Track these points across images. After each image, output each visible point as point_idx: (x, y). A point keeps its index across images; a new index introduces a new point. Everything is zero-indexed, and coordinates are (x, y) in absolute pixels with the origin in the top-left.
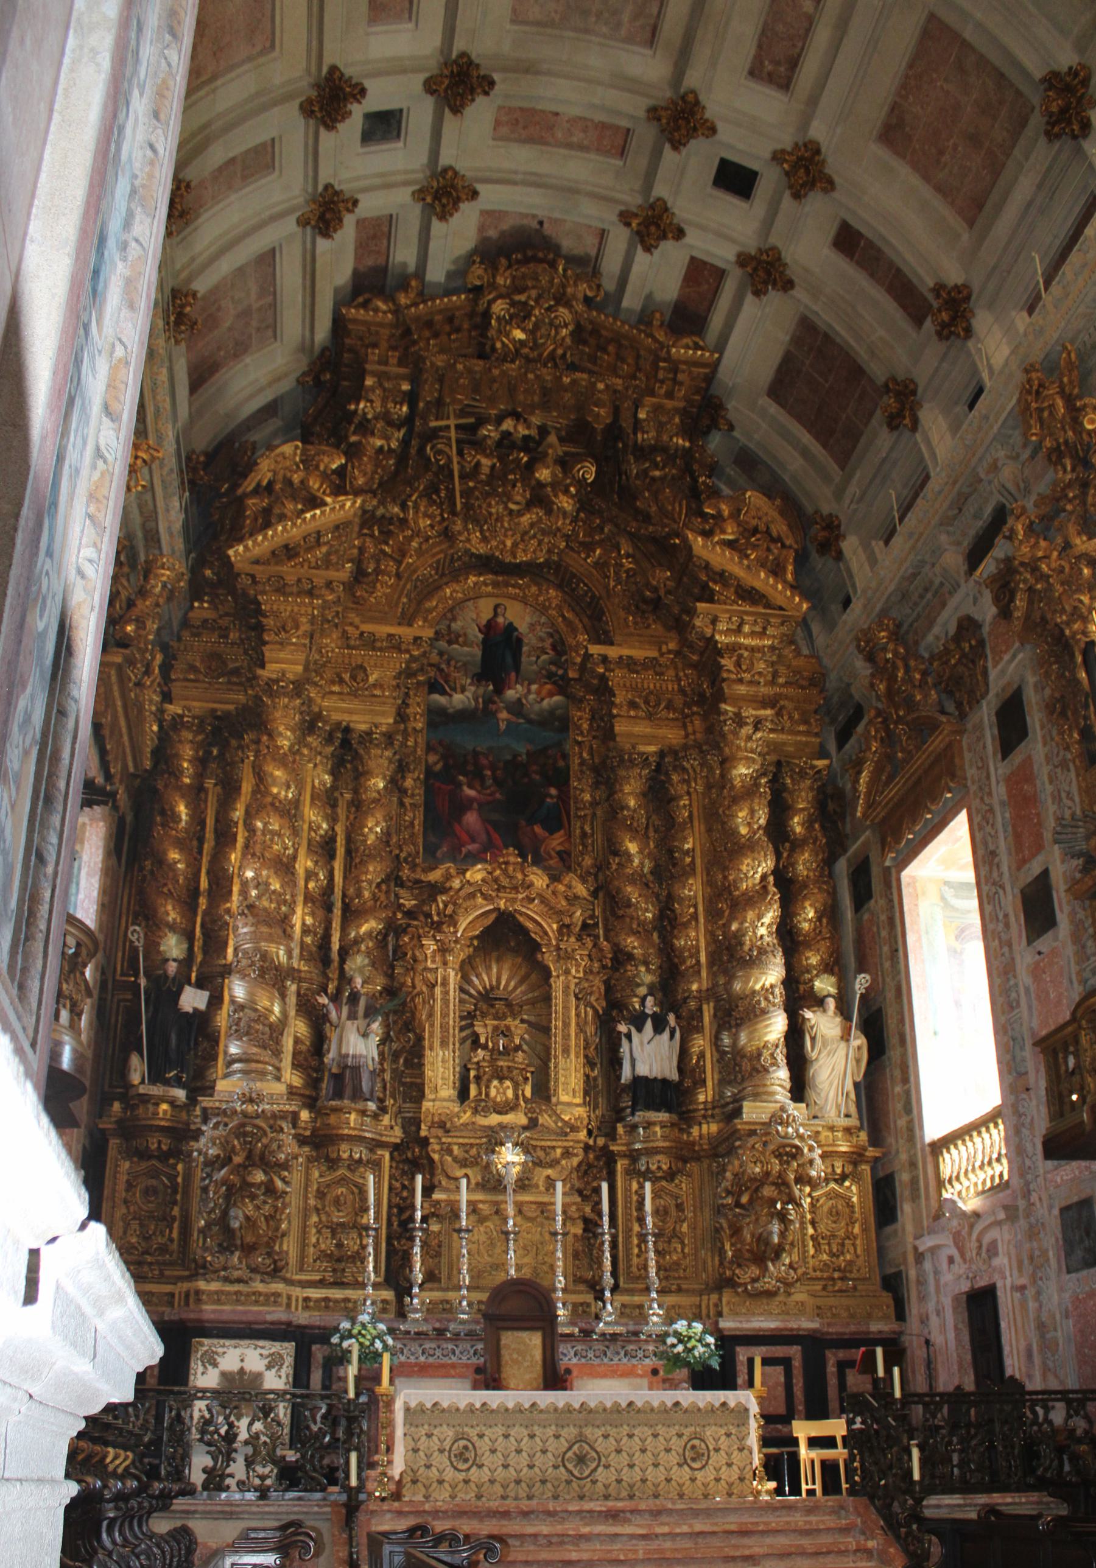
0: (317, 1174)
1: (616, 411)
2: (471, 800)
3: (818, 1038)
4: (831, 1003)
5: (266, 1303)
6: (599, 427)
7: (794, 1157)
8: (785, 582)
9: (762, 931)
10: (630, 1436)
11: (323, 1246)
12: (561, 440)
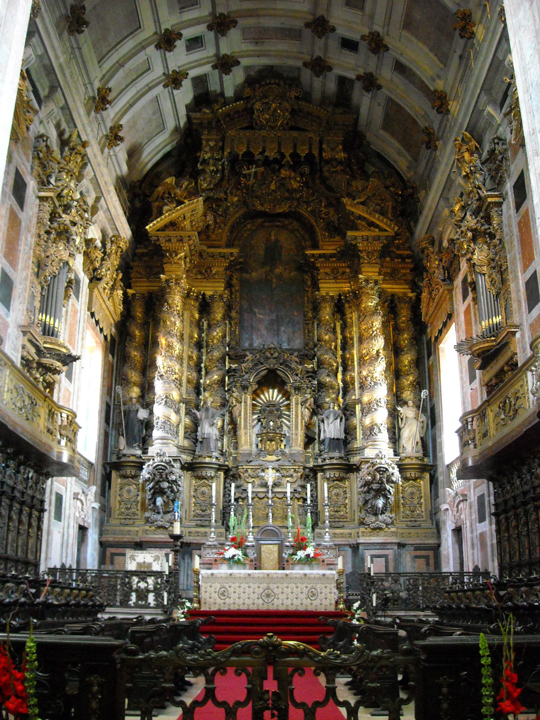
0: (194, 482)
1: (310, 145)
2: (260, 320)
3: (404, 418)
4: (410, 403)
7: (385, 472)
8: (388, 218)
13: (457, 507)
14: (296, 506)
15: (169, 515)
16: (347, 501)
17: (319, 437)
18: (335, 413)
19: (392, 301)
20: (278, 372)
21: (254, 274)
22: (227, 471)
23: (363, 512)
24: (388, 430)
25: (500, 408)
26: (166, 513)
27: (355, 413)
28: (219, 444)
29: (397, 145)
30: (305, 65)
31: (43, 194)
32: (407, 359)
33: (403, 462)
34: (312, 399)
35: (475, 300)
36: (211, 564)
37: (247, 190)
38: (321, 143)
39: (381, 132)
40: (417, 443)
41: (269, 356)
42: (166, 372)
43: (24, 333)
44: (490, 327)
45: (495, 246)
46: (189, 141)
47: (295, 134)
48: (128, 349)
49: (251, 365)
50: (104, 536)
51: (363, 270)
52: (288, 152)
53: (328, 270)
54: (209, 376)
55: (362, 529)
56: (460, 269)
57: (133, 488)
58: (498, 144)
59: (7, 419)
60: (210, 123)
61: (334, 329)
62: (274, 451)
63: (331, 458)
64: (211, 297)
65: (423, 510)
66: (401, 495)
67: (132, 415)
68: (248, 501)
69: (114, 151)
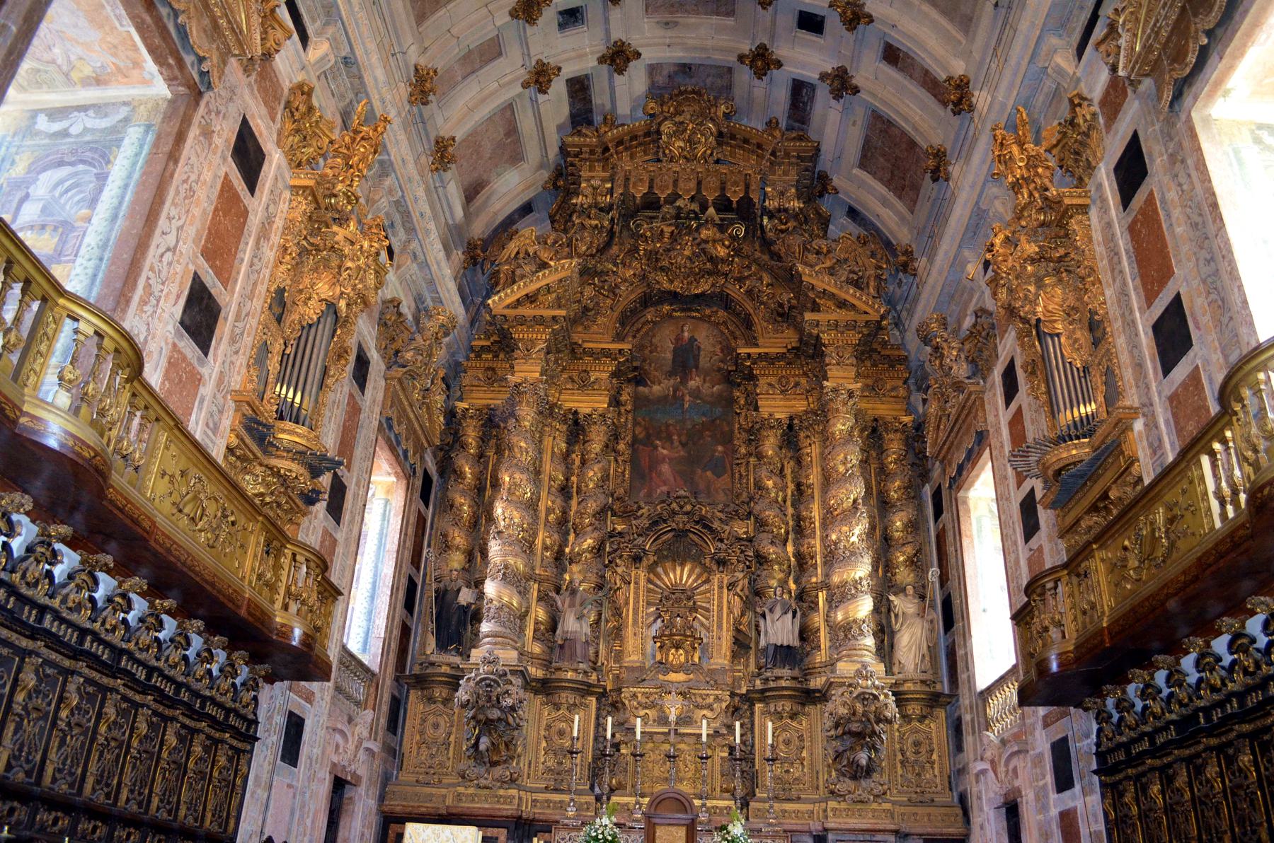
1: (747, 187)
2: (664, 457)
4: (910, 589)
5: (505, 803)
6: (734, 200)
11: (549, 764)
12: (718, 211)
15: (499, 768)
17: (757, 643)
18: (784, 604)
21: (656, 388)
22: (602, 695)
26: (494, 764)
27: (817, 604)
28: (591, 650)
30: (741, 58)
31: (297, 182)
34: (746, 581)
38: (764, 182)
42: (507, 527)
44: (1075, 422)
48: (450, 494)
49: (647, 523)
50: (386, 803)
54: (580, 540)
55: (832, 804)
58: (1080, 105)
59: (146, 524)
61: (782, 470)
63: (778, 678)
65: (935, 775)
66: (897, 746)
67: (449, 597)
69: (442, 181)
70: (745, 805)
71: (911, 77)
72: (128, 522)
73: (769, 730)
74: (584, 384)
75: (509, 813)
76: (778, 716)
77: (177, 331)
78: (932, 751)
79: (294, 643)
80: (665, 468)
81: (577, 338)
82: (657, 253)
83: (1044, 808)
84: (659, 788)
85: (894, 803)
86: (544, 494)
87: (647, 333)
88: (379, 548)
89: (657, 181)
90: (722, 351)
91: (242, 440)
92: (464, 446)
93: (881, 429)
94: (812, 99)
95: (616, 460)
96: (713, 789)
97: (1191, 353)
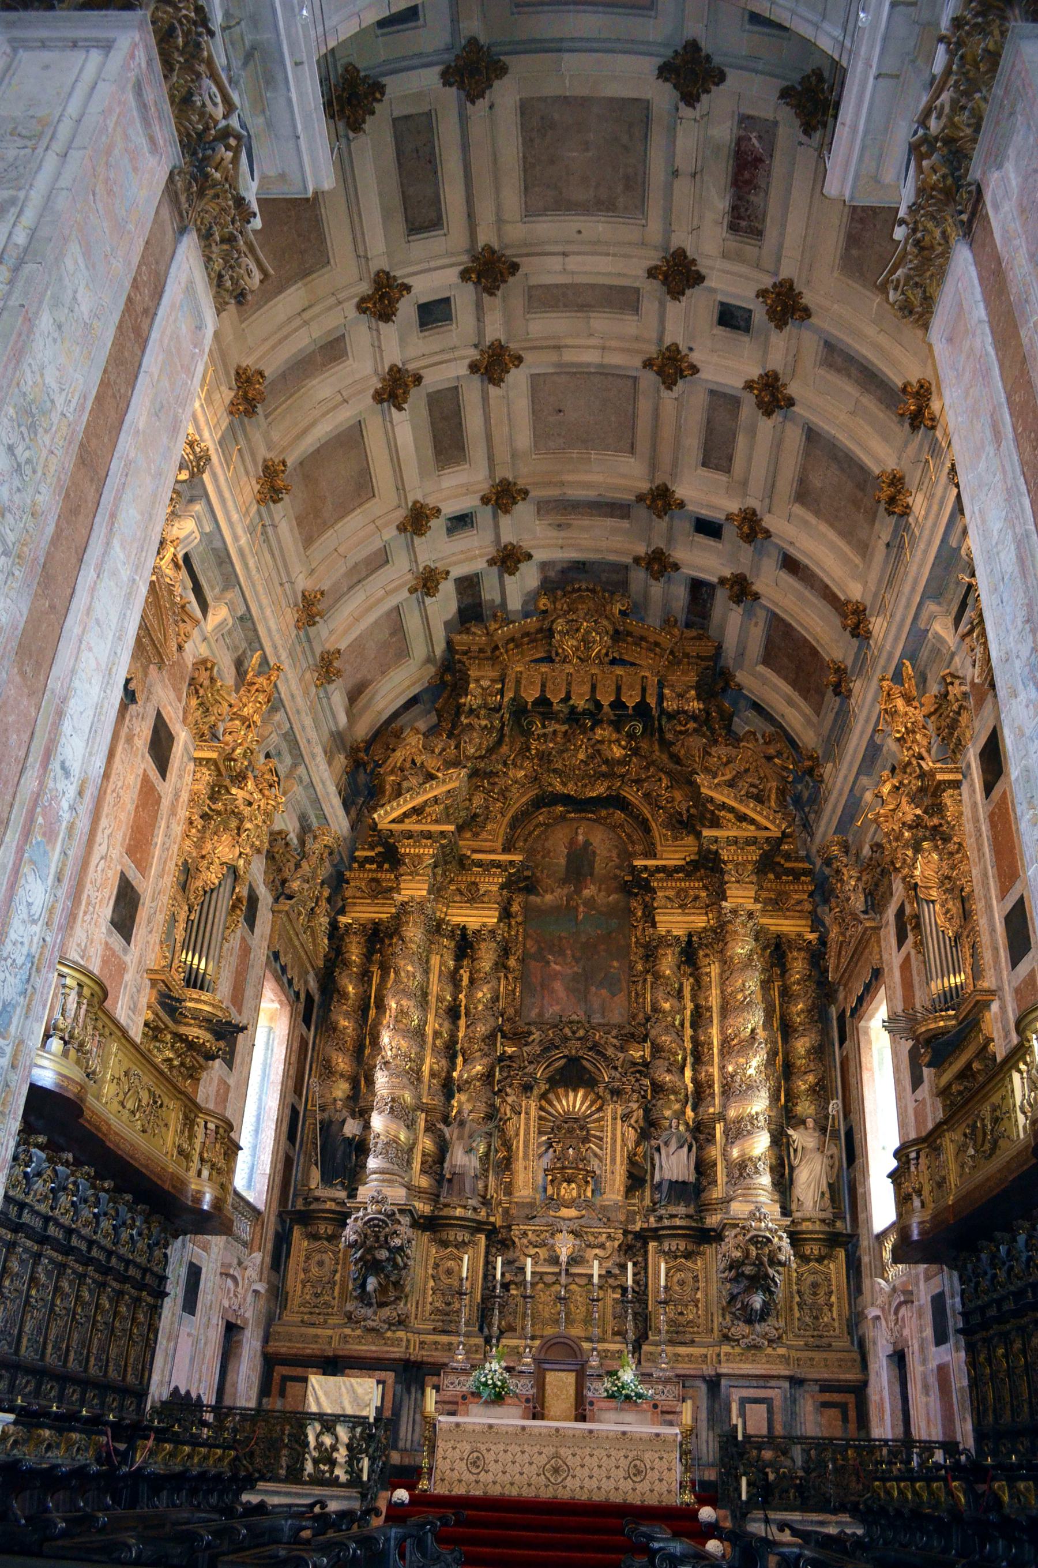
1: (644, 690)
2: (556, 975)
3: (800, 1149)
4: (810, 1122)
6: (631, 704)
9: (751, 1071)
10: (591, 1456)
13: (896, 1313)
14: (609, 1302)
16: (699, 1295)
18: (680, 1137)
19: (778, 946)
20: (585, 1062)
21: (549, 897)
22: (492, 1232)
23: (728, 1317)
24: (772, 1169)
25: (965, 1135)
26: (382, 1305)
27: (714, 1136)
28: (480, 1185)
29: (788, 689)
30: (637, 560)
32: (801, 1045)
33: (799, 1228)
34: (641, 1112)
35: (920, 945)
36: (456, 1403)
37: (541, 759)
38: (661, 685)
39: (761, 668)
40: (823, 1193)
41: (570, 1034)
42: (395, 1057)
43: (154, 983)
45: (951, 854)
46: (448, 678)
47: (619, 671)
48: (333, 1016)
49: (538, 1049)
51: (729, 893)
52: (606, 699)
53: (671, 893)
55: (726, 1349)
56: (891, 894)
57: (328, 1258)
58: (952, 683)
59: (104, 1129)
60: (481, 651)
61: (680, 990)
62: (573, 1200)
63: (672, 1216)
64: (477, 933)
65: (834, 1317)
66: (795, 1287)
67: (334, 1128)
68: (525, 1288)
69: (326, 692)
70: (637, 1347)
71: (812, 587)
72: (93, 1130)
73: (661, 1270)
74: (473, 897)
75: (397, 1356)
76: (671, 1255)
77: (109, 931)
78: (831, 1292)
79: (205, 1207)
80: (558, 986)
81: (466, 845)
82: (550, 754)
83: (924, 1361)
84: (549, 1331)
85: (789, 1347)
86: (431, 1017)
87: (539, 836)
88: (263, 1079)
89: (549, 684)
90: (619, 855)
91: (157, 1015)
92: (346, 964)
93: (785, 947)
94: (712, 596)
95: (506, 978)
96: (605, 1332)
97: (1030, 955)
